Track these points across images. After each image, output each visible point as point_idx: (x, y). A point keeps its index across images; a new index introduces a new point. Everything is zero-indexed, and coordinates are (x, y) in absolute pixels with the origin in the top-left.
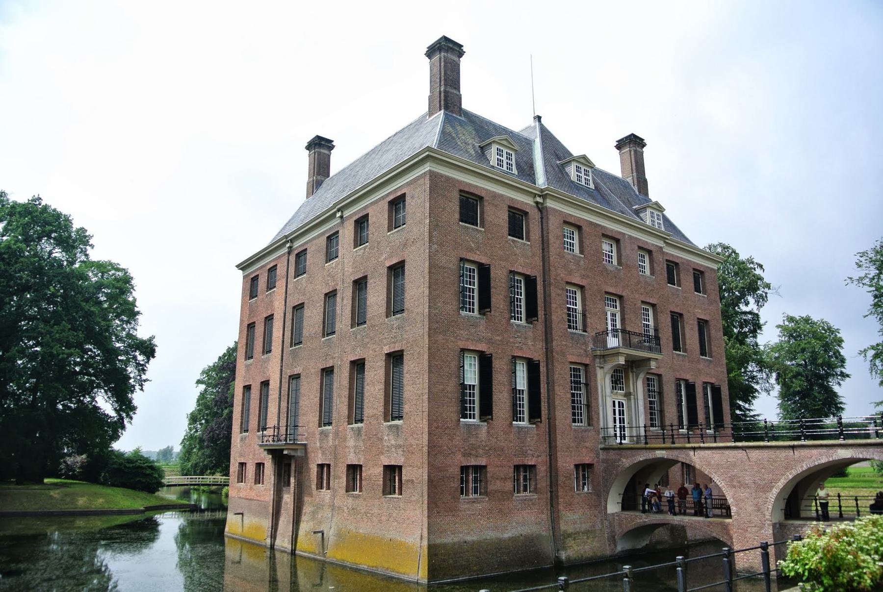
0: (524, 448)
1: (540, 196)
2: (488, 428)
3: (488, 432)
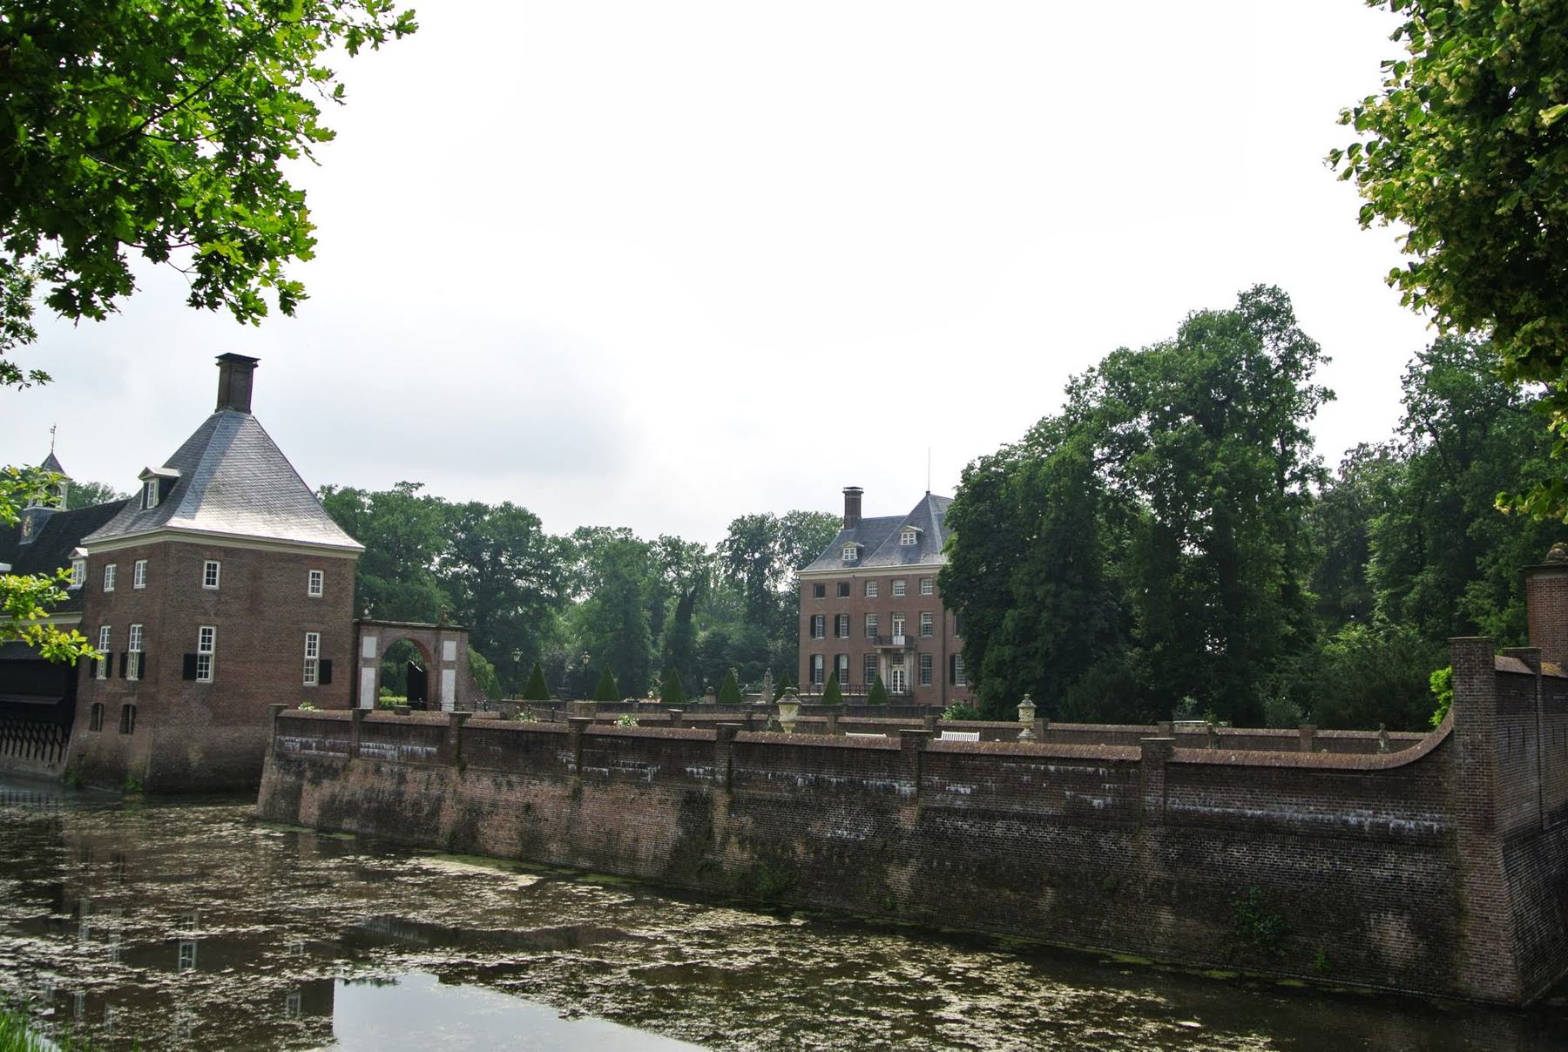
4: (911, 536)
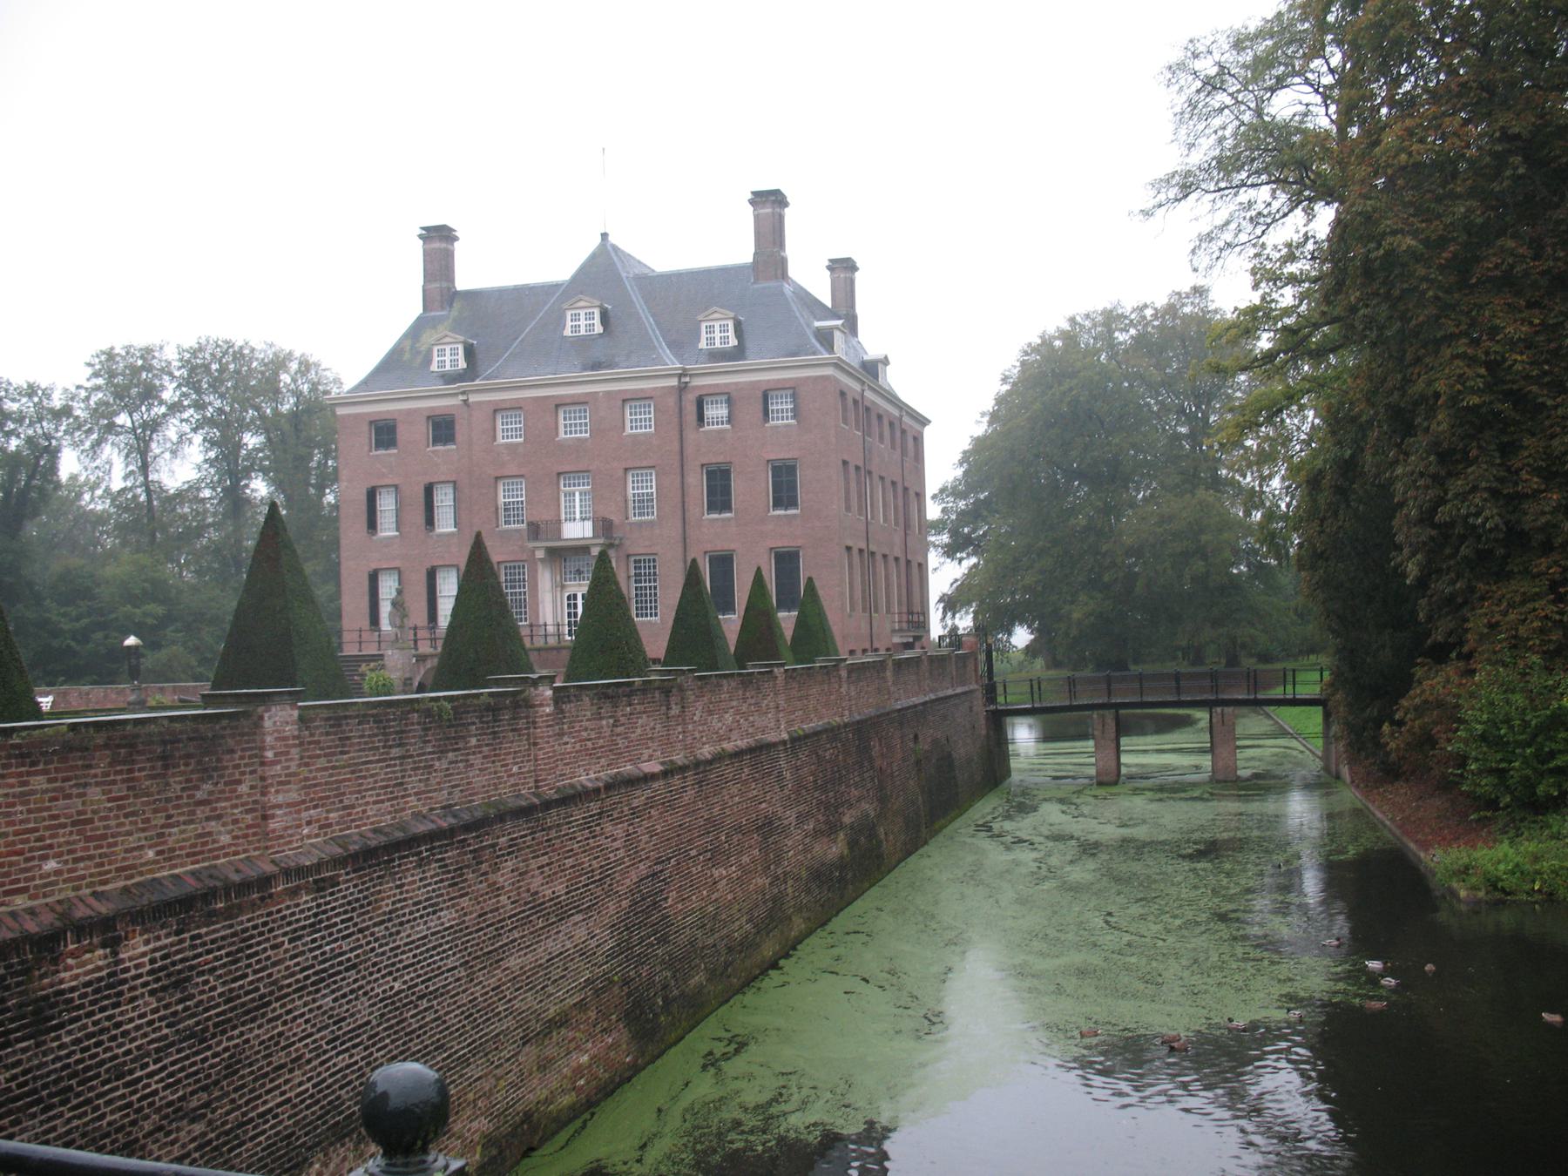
4: (589, 316)
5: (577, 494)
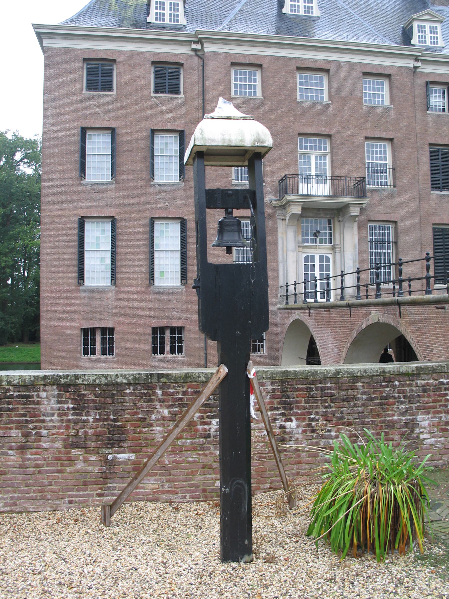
0: (166, 310)
1: (195, 42)
2: (117, 292)
3: (117, 296)
5: (313, 157)
